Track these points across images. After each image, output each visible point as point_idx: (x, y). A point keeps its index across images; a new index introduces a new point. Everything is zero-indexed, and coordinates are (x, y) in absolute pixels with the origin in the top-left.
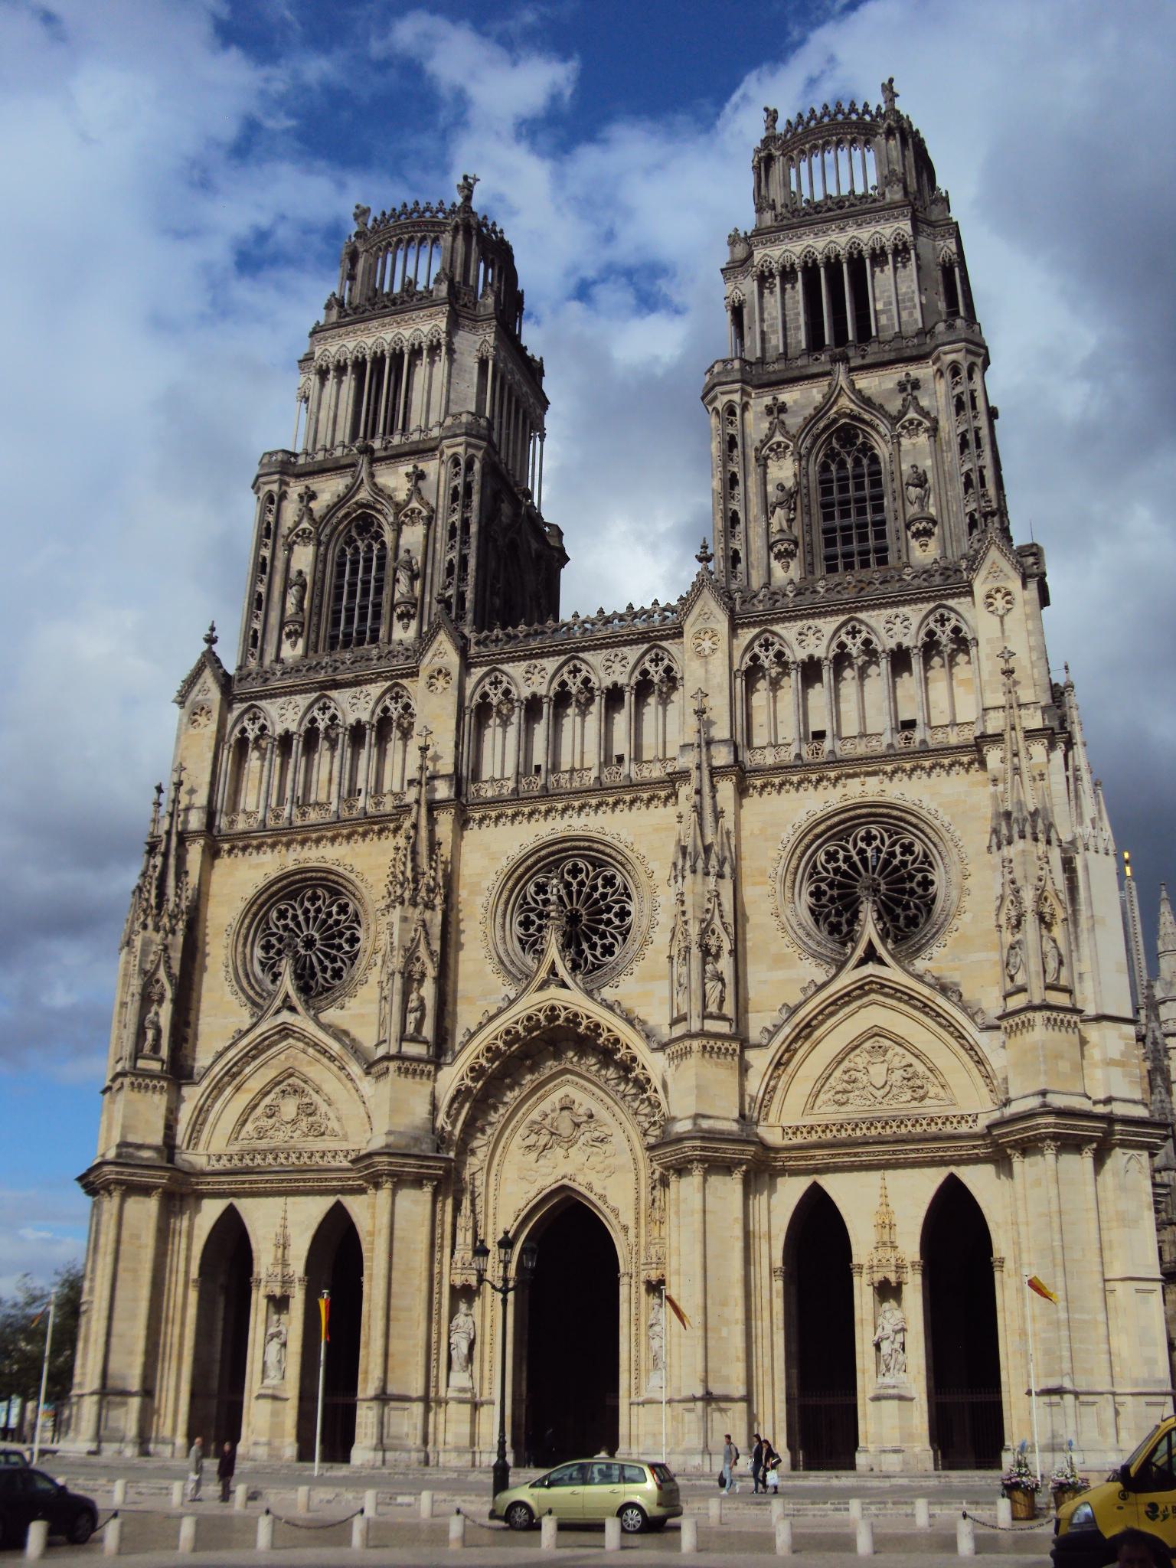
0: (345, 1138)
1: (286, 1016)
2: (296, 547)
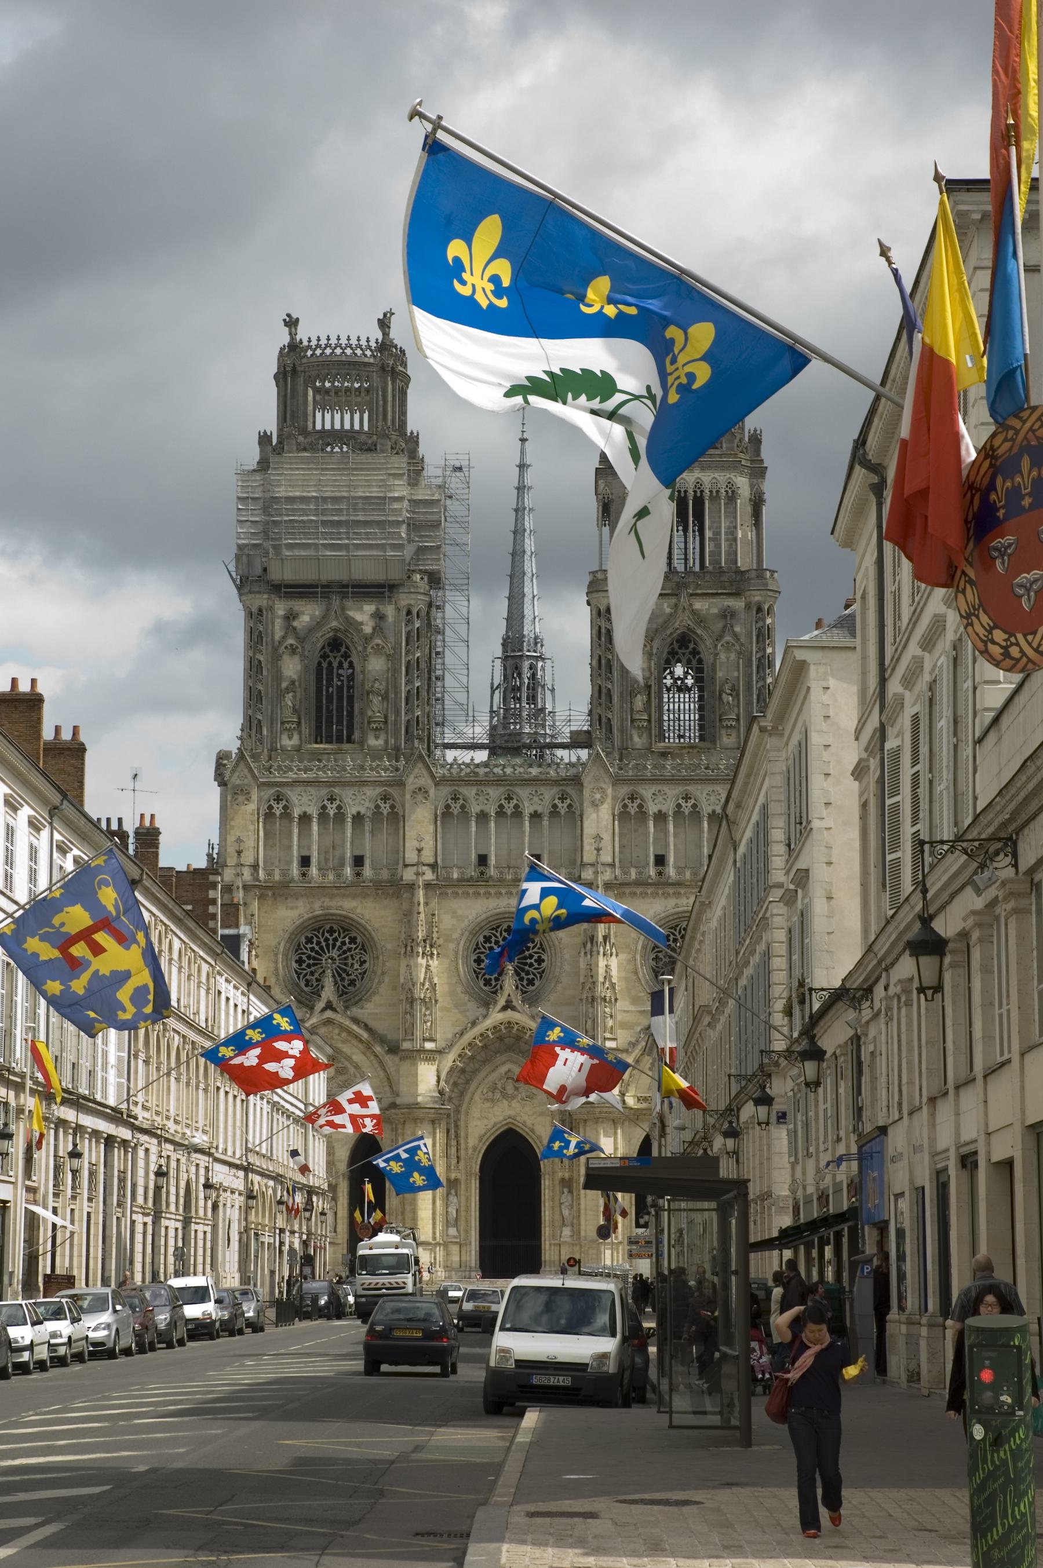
1: (329, 1014)
2: (285, 657)
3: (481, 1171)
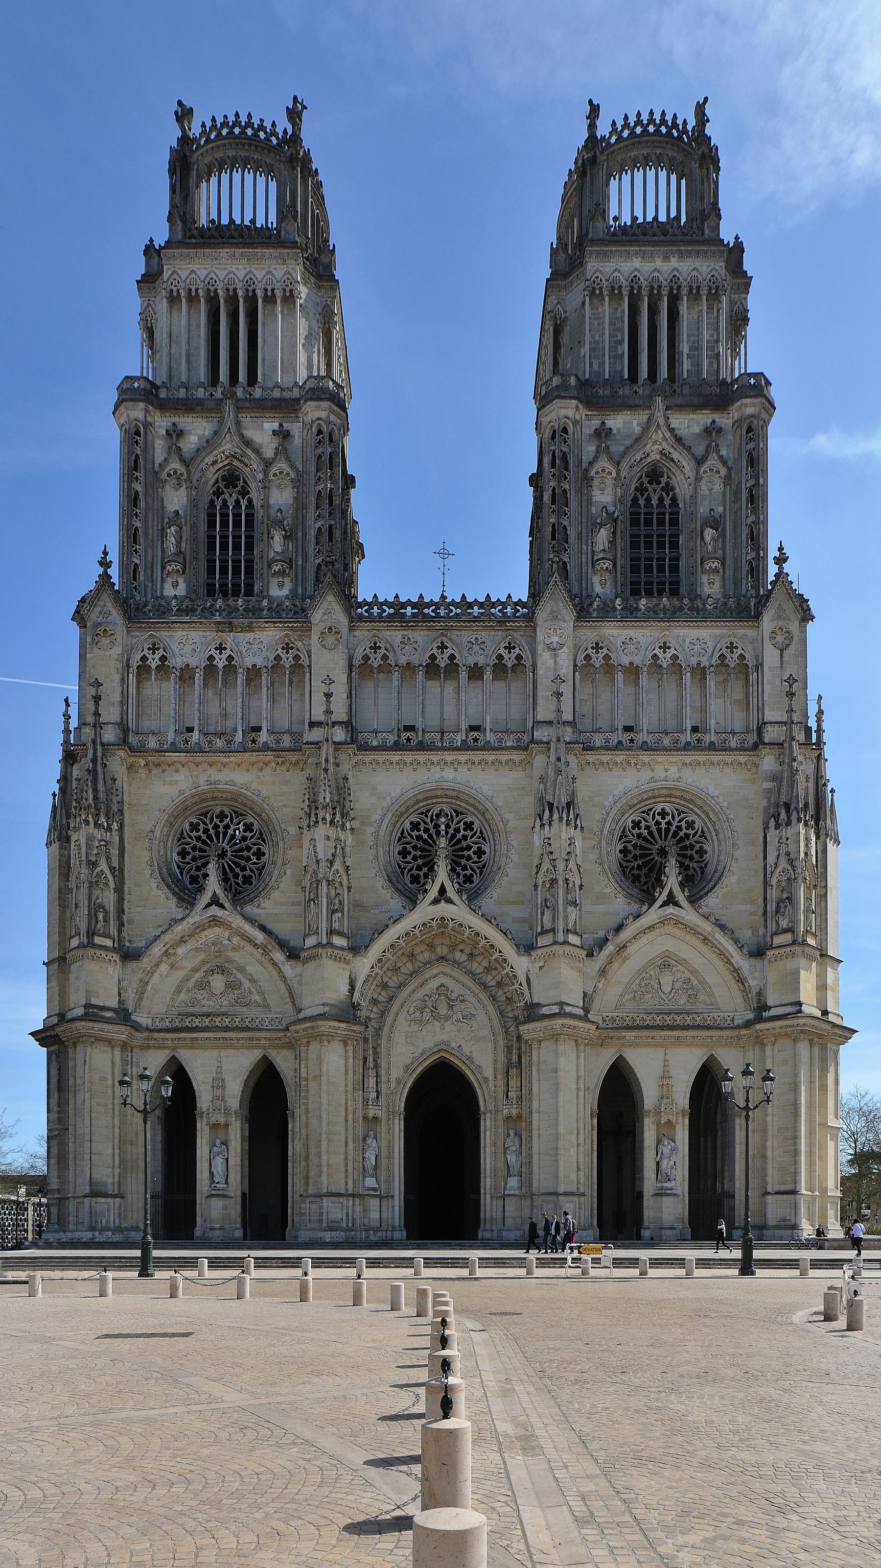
0: (266, 1006)
1: (214, 910)
3: (406, 1109)
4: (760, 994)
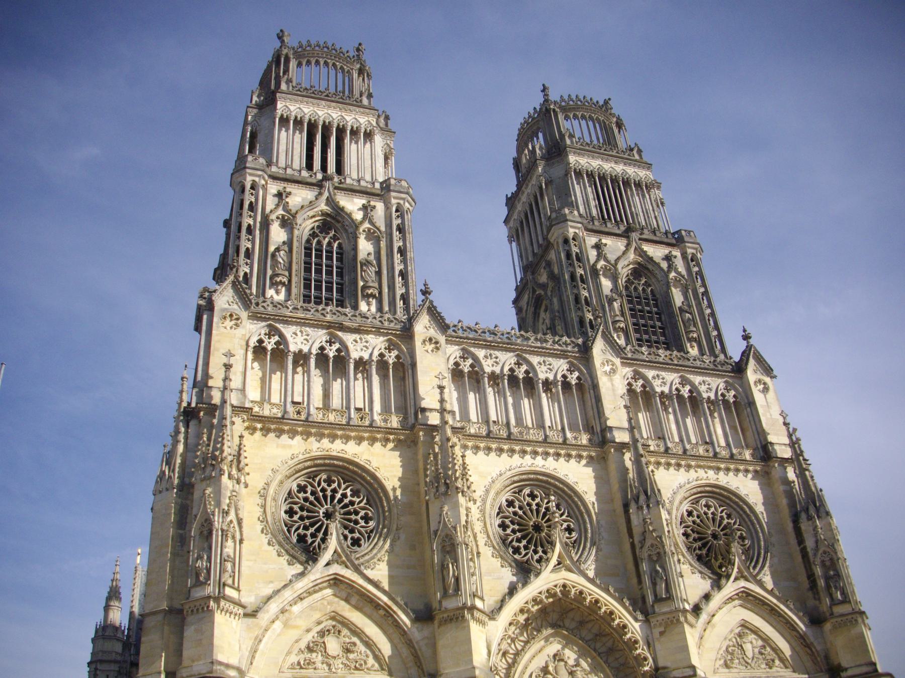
1: (336, 569)
4: (827, 657)
